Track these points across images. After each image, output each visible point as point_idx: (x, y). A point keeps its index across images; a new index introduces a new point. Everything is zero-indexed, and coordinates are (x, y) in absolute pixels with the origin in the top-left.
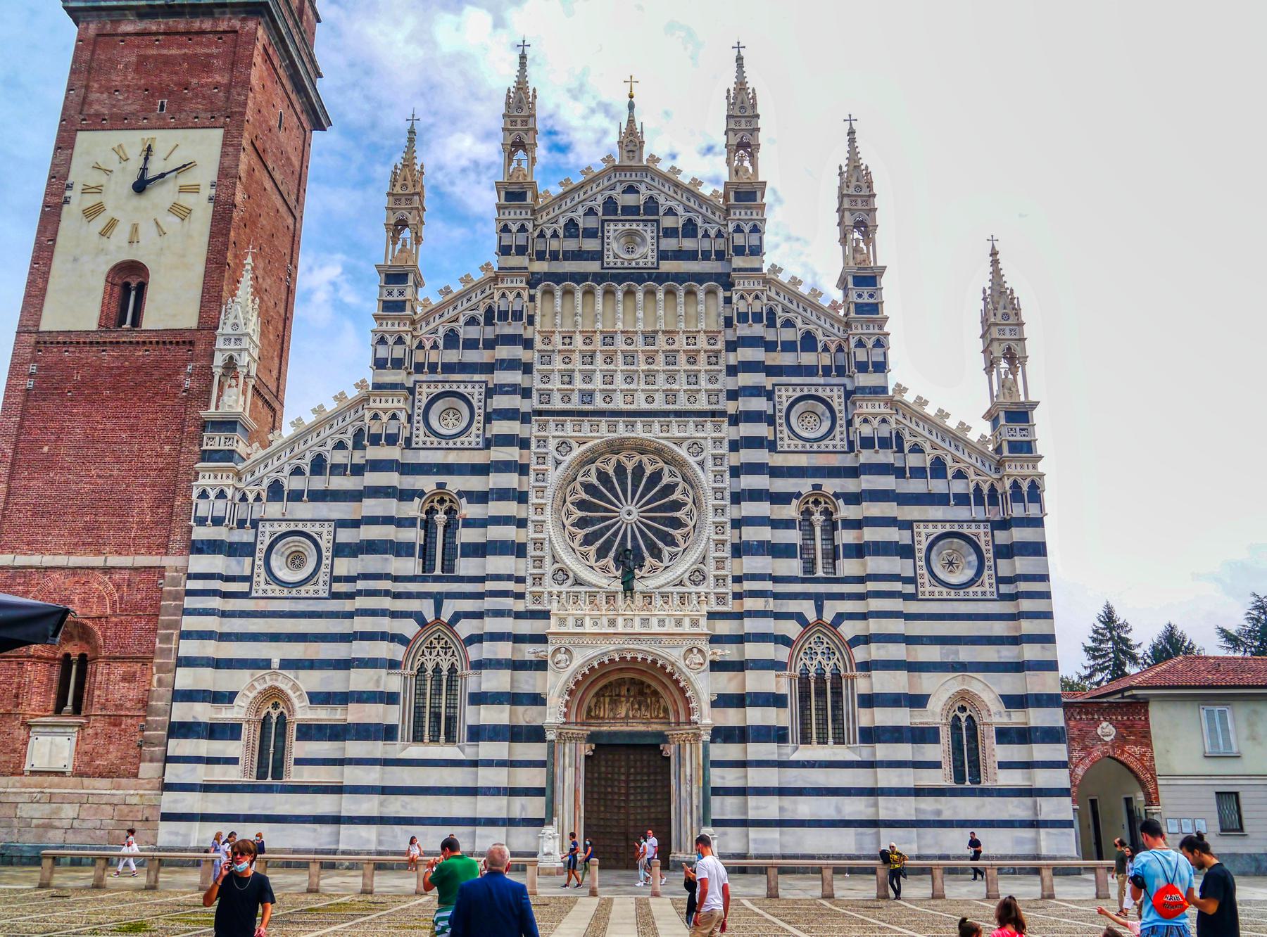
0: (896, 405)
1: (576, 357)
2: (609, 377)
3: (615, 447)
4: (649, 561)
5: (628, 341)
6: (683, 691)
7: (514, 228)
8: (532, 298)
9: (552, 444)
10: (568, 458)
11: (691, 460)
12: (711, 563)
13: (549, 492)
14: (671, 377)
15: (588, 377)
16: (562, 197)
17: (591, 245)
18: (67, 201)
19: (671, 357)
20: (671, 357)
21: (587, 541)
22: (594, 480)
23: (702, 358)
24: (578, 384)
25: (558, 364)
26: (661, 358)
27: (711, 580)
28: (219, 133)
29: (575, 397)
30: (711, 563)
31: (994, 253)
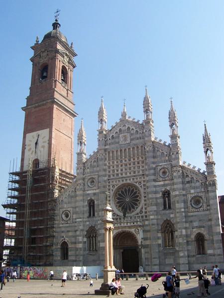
0: (183, 167)
1: (115, 167)
2: (122, 170)
3: (124, 185)
4: (128, 211)
5: (126, 161)
6: (135, 238)
7: (101, 140)
8: (106, 154)
9: (111, 186)
10: (114, 189)
11: (139, 186)
12: (144, 209)
13: (111, 197)
14: (134, 168)
15: (117, 171)
16: (111, 130)
17: (117, 140)
18: (25, 148)
19: (134, 163)
20: (134, 163)
21: (119, 207)
22: (120, 193)
23: (140, 162)
24: (116, 171)
25: (111, 167)
26: (132, 164)
27: (144, 213)
28: (49, 129)
29: (115, 175)
30: (144, 209)
31: (205, 125)
